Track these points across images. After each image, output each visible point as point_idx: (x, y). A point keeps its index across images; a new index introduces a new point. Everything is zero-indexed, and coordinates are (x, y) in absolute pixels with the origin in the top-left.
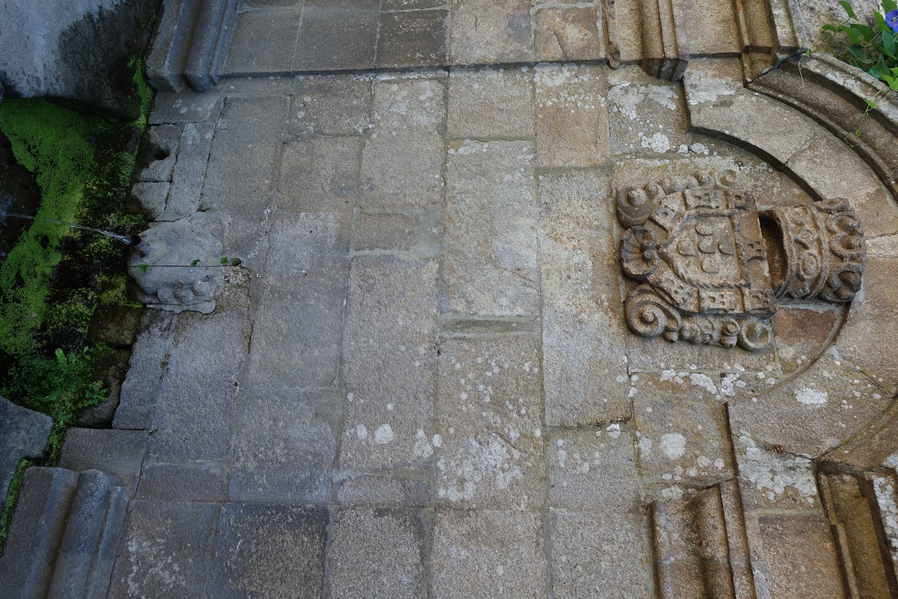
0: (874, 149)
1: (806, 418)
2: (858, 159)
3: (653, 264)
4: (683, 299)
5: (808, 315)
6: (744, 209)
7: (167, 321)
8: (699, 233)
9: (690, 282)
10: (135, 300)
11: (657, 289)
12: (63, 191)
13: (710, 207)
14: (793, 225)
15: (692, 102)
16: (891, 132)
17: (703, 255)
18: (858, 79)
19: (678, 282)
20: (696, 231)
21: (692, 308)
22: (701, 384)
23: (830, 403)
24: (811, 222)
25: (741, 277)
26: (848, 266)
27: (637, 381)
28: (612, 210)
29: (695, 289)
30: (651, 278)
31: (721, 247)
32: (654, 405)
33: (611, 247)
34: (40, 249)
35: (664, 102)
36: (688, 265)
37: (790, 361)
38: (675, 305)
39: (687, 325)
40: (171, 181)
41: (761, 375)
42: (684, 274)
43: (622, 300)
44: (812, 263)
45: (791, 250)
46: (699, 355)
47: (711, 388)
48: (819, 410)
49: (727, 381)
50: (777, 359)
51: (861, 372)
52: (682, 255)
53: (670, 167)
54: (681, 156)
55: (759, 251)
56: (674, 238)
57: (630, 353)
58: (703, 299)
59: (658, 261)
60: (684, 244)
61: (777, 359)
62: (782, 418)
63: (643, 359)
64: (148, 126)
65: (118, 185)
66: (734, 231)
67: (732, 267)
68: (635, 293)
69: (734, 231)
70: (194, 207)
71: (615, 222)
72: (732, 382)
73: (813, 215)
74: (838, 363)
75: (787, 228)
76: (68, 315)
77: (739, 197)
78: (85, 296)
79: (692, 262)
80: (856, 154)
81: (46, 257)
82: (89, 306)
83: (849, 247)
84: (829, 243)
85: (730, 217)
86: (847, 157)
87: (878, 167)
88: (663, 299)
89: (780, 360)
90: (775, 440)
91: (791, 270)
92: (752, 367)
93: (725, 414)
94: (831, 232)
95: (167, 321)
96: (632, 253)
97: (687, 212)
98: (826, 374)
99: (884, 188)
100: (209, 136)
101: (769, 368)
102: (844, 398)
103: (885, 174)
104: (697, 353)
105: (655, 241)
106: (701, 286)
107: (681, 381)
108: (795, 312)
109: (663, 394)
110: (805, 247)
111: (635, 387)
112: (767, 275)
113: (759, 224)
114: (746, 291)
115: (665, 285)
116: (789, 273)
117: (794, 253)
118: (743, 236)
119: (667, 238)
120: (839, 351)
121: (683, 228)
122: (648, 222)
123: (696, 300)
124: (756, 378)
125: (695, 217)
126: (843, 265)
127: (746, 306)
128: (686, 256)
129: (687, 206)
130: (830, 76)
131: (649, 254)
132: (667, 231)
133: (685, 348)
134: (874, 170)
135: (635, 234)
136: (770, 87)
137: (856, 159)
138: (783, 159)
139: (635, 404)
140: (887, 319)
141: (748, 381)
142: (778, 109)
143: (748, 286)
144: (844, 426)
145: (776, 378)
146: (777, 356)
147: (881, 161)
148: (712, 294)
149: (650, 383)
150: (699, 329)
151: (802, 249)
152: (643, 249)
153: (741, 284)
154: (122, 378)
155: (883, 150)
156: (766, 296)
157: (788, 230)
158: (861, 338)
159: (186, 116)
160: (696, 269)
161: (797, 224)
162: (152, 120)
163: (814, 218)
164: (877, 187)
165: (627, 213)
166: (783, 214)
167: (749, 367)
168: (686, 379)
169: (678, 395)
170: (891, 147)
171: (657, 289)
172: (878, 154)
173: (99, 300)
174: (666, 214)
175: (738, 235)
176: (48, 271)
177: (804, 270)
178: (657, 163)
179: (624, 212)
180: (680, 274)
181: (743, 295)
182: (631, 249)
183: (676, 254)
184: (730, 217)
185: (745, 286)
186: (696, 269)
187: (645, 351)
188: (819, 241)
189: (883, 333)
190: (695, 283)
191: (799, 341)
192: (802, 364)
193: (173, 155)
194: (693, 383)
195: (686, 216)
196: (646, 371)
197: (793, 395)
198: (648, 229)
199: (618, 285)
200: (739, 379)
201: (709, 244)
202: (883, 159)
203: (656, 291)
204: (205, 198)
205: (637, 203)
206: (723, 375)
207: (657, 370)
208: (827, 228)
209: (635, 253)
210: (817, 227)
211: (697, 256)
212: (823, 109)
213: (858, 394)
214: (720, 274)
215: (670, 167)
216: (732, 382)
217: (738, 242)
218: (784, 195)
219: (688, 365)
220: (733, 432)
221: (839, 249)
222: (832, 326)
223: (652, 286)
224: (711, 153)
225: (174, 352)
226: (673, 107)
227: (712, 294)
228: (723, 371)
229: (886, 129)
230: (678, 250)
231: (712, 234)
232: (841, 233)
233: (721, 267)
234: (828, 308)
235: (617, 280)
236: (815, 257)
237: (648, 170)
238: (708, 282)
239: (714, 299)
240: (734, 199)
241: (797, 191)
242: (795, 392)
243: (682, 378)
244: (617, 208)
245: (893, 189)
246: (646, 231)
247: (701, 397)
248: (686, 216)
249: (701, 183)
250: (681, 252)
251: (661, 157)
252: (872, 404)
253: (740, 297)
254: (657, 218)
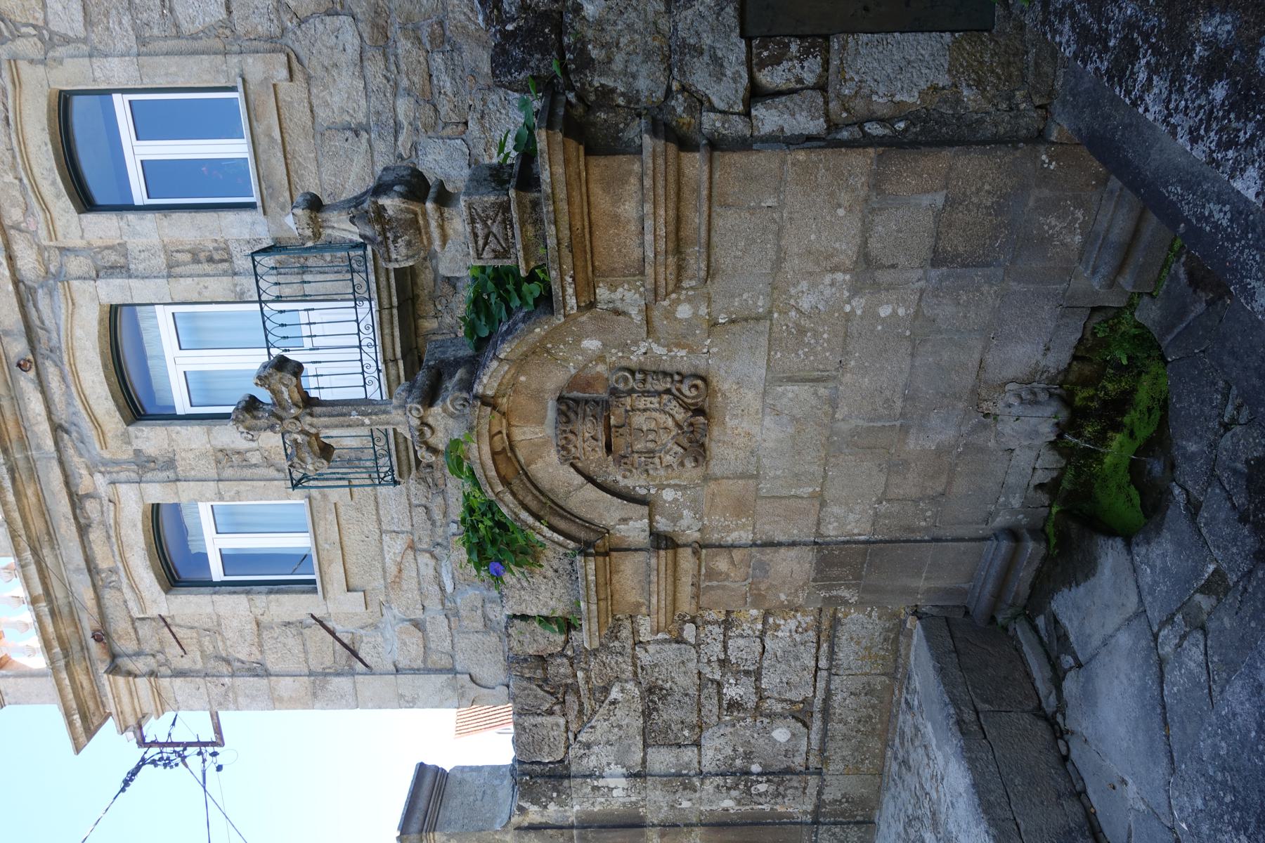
2: (539, 485)
7: (1044, 377)
9: (665, 413)
10: (1068, 390)
12: (1116, 466)
15: (646, 521)
18: (544, 537)
19: (673, 412)
21: (665, 397)
22: (661, 348)
23: (580, 341)
32: (695, 335)
34: (1135, 430)
35: (663, 520)
38: (676, 398)
40: (1034, 469)
41: (620, 354)
47: (654, 346)
49: (643, 350)
53: (664, 479)
54: (655, 486)
64: (1050, 506)
65: (1077, 468)
70: (1017, 452)
76: (1120, 381)
78: (1106, 394)
81: (1132, 422)
82: (1104, 387)
95: (1044, 377)
98: (580, 358)
100: (1002, 499)
101: (614, 358)
107: (674, 349)
115: (682, 410)
121: (665, 445)
124: (623, 352)
128: (666, 428)
129: (660, 458)
130: (561, 538)
136: (593, 530)
138: (590, 486)
142: (588, 516)
143: (627, 411)
154: (1081, 340)
159: (1019, 513)
162: (1047, 510)
173: (1097, 390)
176: (1133, 412)
178: (672, 482)
184: (633, 452)
187: (696, 367)
193: (1032, 486)
197: (604, 345)
204: (1008, 458)
205: (692, 459)
206: (645, 353)
212: (562, 517)
213: (562, 346)
215: (664, 479)
221: (571, 436)
224: (634, 488)
225: (1040, 357)
226: (658, 517)
237: (679, 477)
238: (654, 413)
249: (647, 471)
251: (669, 486)
254: (682, 451)
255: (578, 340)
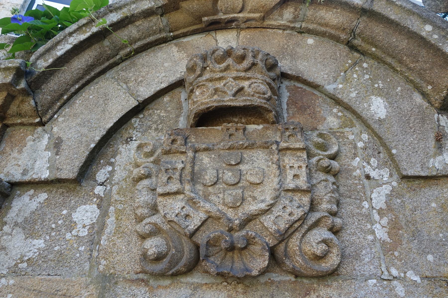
0: (139, 39)
1: (400, 113)
2: (144, 54)
3: (254, 238)
4: (298, 207)
5: (292, 102)
6: (186, 138)
8: (215, 183)
9: (277, 198)
11: (286, 236)
13: (183, 169)
14: (216, 97)
15: (45, 175)
16: (128, 24)
17: (242, 181)
18: (71, 34)
19: (277, 211)
20: (212, 185)
21: (306, 199)
22: (384, 199)
23: (380, 95)
24: (213, 83)
25: (268, 148)
26: (261, 60)
27: (398, 269)
28: (167, 282)
29: (283, 194)
30: (272, 242)
31: (233, 163)
32: (424, 253)
33: (220, 287)
35: (34, 205)
36: (254, 198)
37: (340, 120)
38: (303, 219)
39: (325, 206)
41: (360, 145)
42: (268, 203)
43: (293, 279)
44: (259, 86)
45: (245, 100)
46: (350, 197)
47: (386, 190)
48: (390, 103)
49: (373, 174)
50: (341, 130)
51: (345, 72)
52: (242, 203)
53: (120, 207)
54: (108, 194)
55: (237, 129)
56: (219, 210)
57: (362, 275)
58: (297, 187)
59: (250, 231)
60: (229, 199)
61: (341, 130)
62: (406, 132)
63: (367, 260)
66: (213, 149)
67: (255, 155)
68: (288, 263)
69: (213, 149)
71: (184, 279)
72: (374, 170)
73: (207, 80)
74: (341, 86)
75: (219, 101)
77: (174, 141)
79: (250, 193)
80: (139, 54)
83: (243, 58)
84: (237, 71)
85: (196, 151)
86: (141, 60)
87: (156, 41)
88: (296, 230)
89: (342, 128)
90: (430, 140)
91: (265, 103)
92: (353, 151)
93: (412, 180)
94: (227, 68)
96: (233, 262)
97: (187, 193)
98: (353, 95)
99: (174, 41)
101: (351, 137)
102: (373, 86)
103: (163, 37)
104: (348, 199)
105: (222, 233)
106: (280, 187)
107: (385, 221)
108: (291, 112)
109: (406, 240)
110: (241, 90)
111: (405, 273)
112: (261, 127)
113: (204, 128)
114: (283, 145)
115: (283, 226)
116: (266, 106)
117: (249, 98)
118: (220, 142)
119: (220, 219)
120: (329, 84)
121: (206, 198)
122: (194, 239)
123: (296, 194)
124: (365, 149)
125: (194, 185)
126: (261, 64)
127: (301, 147)
128: (243, 199)
129: (177, 193)
130: (59, 53)
131: (241, 242)
132: (209, 217)
133: (347, 209)
134: (157, 45)
135: (209, 256)
136: (52, 103)
137: (143, 55)
138: (133, 103)
139: (428, 274)
140: (294, 52)
141: (370, 156)
142: (78, 101)
143: (277, 143)
144: (399, 88)
145: (361, 132)
146: (338, 130)
147: (151, 38)
148: (290, 177)
149: (396, 254)
150: (329, 195)
151: (242, 92)
152: (232, 248)
153: (277, 149)
155: (143, 33)
156: (287, 129)
157: (223, 101)
158: (314, 69)
160: (260, 190)
161: (215, 94)
163: (211, 80)
164: (173, 45)
165: (177, 263)
166: (202, 104)
167: (354, 154)
168: (380, 212)
169: (403, 223)
170: (142, 27)
171: (286, 236)
172: (145, 38)
174: (187, 216)
175: (218, 146)
177: (264, 94)
178: (111, 221)
179: (174, 267)
180: (267, 208)
181: (288, 149)
182: (228, 263)
183: (240, 210)
184: (196, 151)
185: (278, 145)
186: (260, 190)
187: (357, 257)
188: (236, 78)
189: (307, 55)
190: (277, 193)
191: (320, 112)
192: (342, 112)
194: (384, 207)
195: (193, 195)
196: (382, 257)
197: (380, 120)
198: (205, 240)
199: (272, 282)
200: (369, 163)
201: (230, 174)
202: (150, 36)
203: (287, 238)
205: (164, 249)
206: (368, 177)
207: (378, 245)
208: (221, 71)
209: (233, 258)
210: (221, 79)
211: (244, 188)
212: (91, 67)
213: (367, 77)
214: (264, 167)
215: (120, 207)
216: (374, 170)
217: (227, 147)
218: (169, 109)
219: (364, 210)
220: (434, 173)
221: (246, 64)
222: (301, 88)
223: (280, 242)
224: (111, 164)
226: (43, 196)
227: (290, 177)
228: (363, 177)
229: (124, 27)
230: (235, 208)
231: (217, 170)
232: (230, 61)
233: (256, 165)
234: (284, 89)
235: (266, 283)
236: (252, 83)
237: (118, 231)
238: (276, 180)
239: (296, 176)
240: (176, 146)
241: (166, 99)
242: (378, 118)
243: (381, 218)
244: (168, 276)
245: (177, 35)
246: (208, 242)
247: (399, 201)
248: (193, 195)
249: (148, 176)
250: (238, 204)
251: (104, 214)
252: (373, 69)
253: (288, 152)
254: (192, 227)
255: (379, 93)
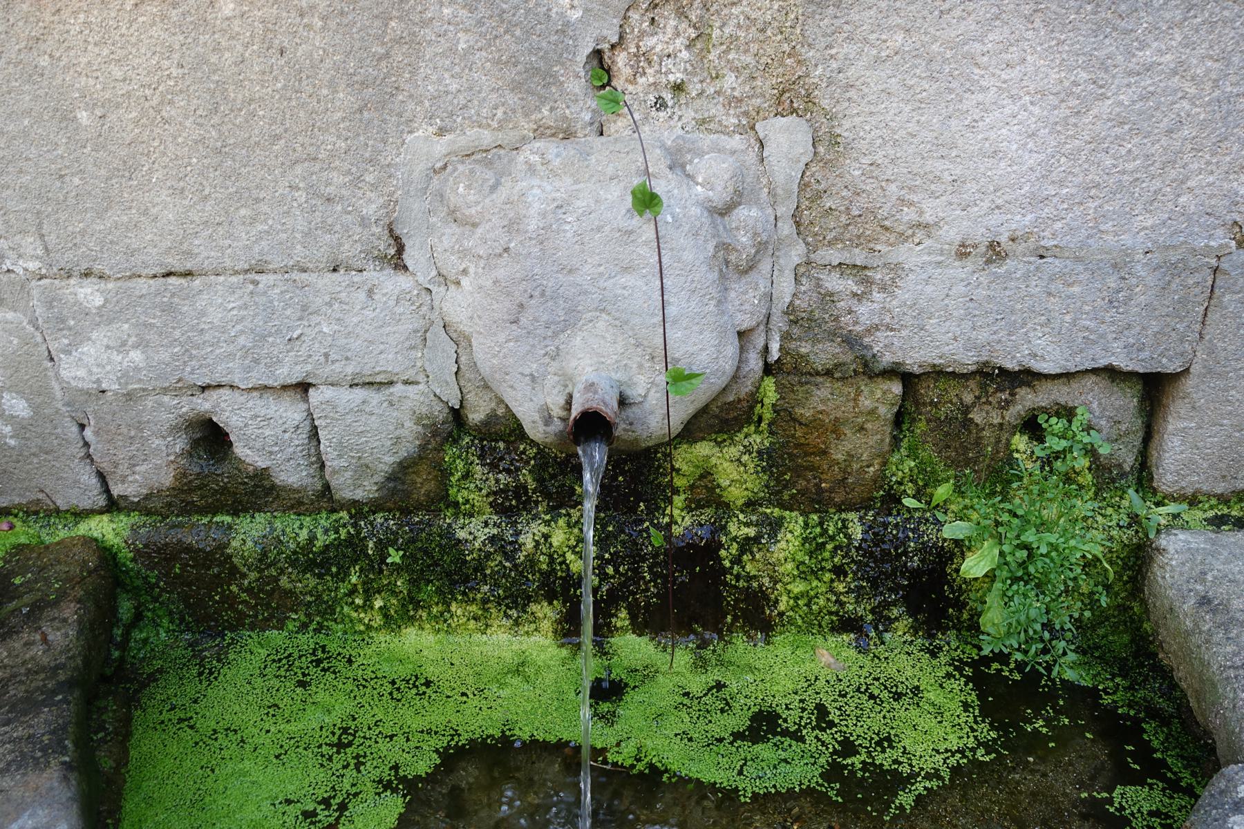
7: (834, 282)
10: (754, 399)
12: (423, 684)
34: (631, 697)
40: (304, 387)
64: (113, 506)
65: (354, 545)
70: (403, 282)
76: (805, 573)
78: (747, 545)
81: (647, 674)
82: (775, 526)
95: (834, 282)
100: (89, 294)
154: (1027, 377)
159: (37, 394)
162: (88, 493)
173: (751, 505)
176: (683, 658)
193: (203, 404)
204: (349, 250)
225: (951, 234)
